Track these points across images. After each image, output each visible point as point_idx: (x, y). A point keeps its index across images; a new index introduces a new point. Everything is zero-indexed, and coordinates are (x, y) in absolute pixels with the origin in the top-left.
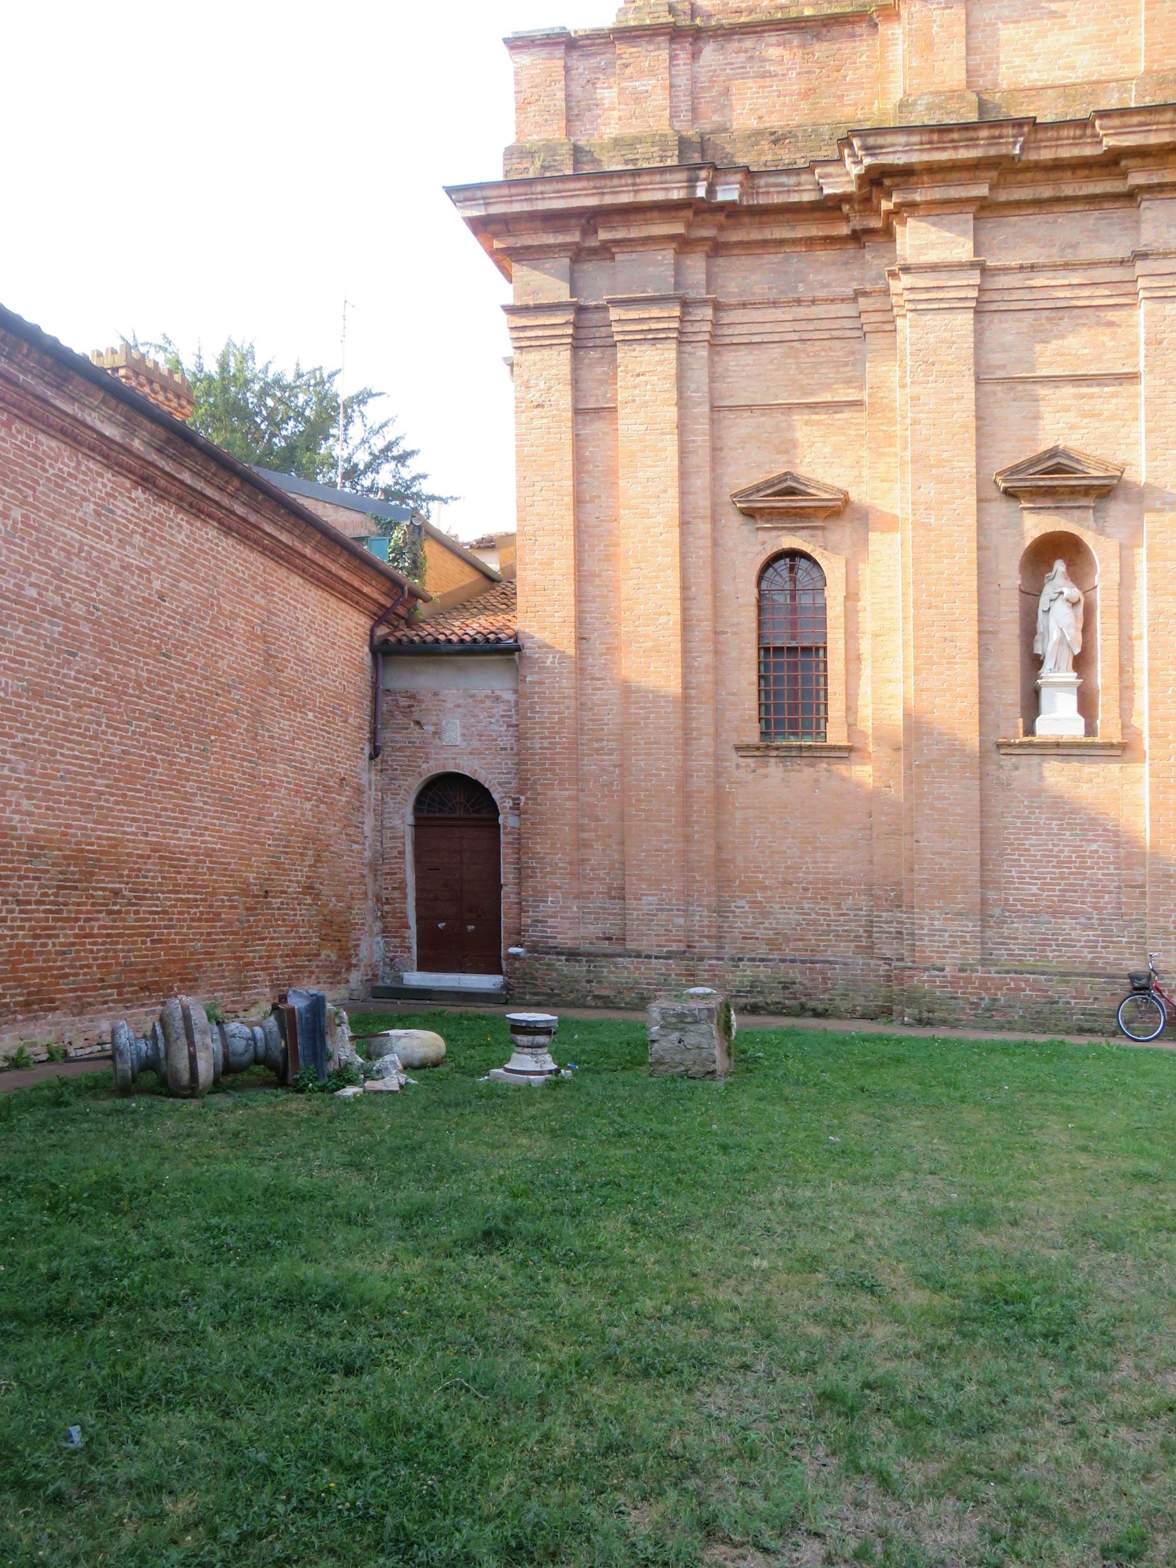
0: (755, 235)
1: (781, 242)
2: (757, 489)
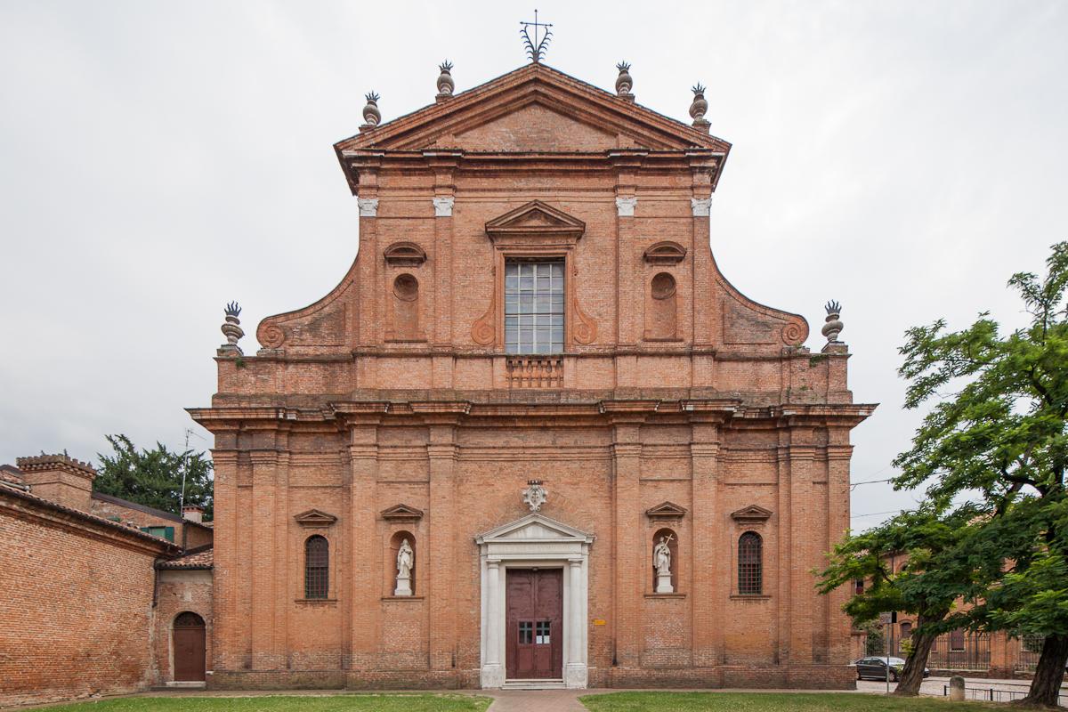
0: (305, 430)
1: (314, 433)
2: (303, 515)
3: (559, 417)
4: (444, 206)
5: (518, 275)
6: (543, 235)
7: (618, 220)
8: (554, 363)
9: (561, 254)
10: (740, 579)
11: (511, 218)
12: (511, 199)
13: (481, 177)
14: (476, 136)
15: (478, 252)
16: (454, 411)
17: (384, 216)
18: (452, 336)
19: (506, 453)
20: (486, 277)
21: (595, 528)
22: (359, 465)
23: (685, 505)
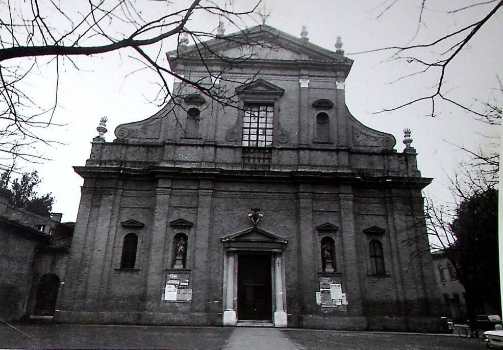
6: (264, 94)
7: (300, 89)
22: (160, 198)
23: (337, 225)
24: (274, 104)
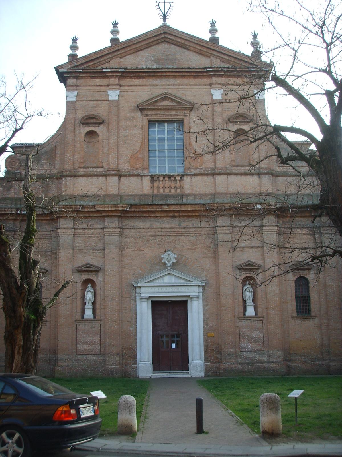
3: (182, 211)
4: (114, 95)
5: (157, 128)
8: (178, 178)
9: (181, 118)
10: (297, 306)
11: (152, 101)
12: (152, 90)
13: (134, 79)
14: (132, 58)
15: (133, 118)
16: (120, 209)
17: (80, 100)
18: (118, 163)
19: (151, 232)
20: (138, 131)
21: (206, 276)
23: (260, 262)
24: (183, 121)
